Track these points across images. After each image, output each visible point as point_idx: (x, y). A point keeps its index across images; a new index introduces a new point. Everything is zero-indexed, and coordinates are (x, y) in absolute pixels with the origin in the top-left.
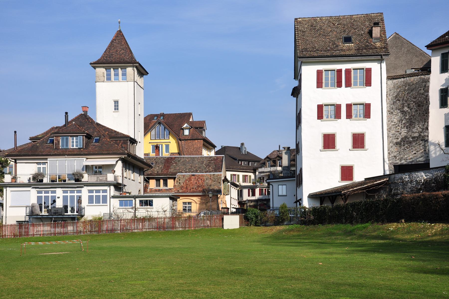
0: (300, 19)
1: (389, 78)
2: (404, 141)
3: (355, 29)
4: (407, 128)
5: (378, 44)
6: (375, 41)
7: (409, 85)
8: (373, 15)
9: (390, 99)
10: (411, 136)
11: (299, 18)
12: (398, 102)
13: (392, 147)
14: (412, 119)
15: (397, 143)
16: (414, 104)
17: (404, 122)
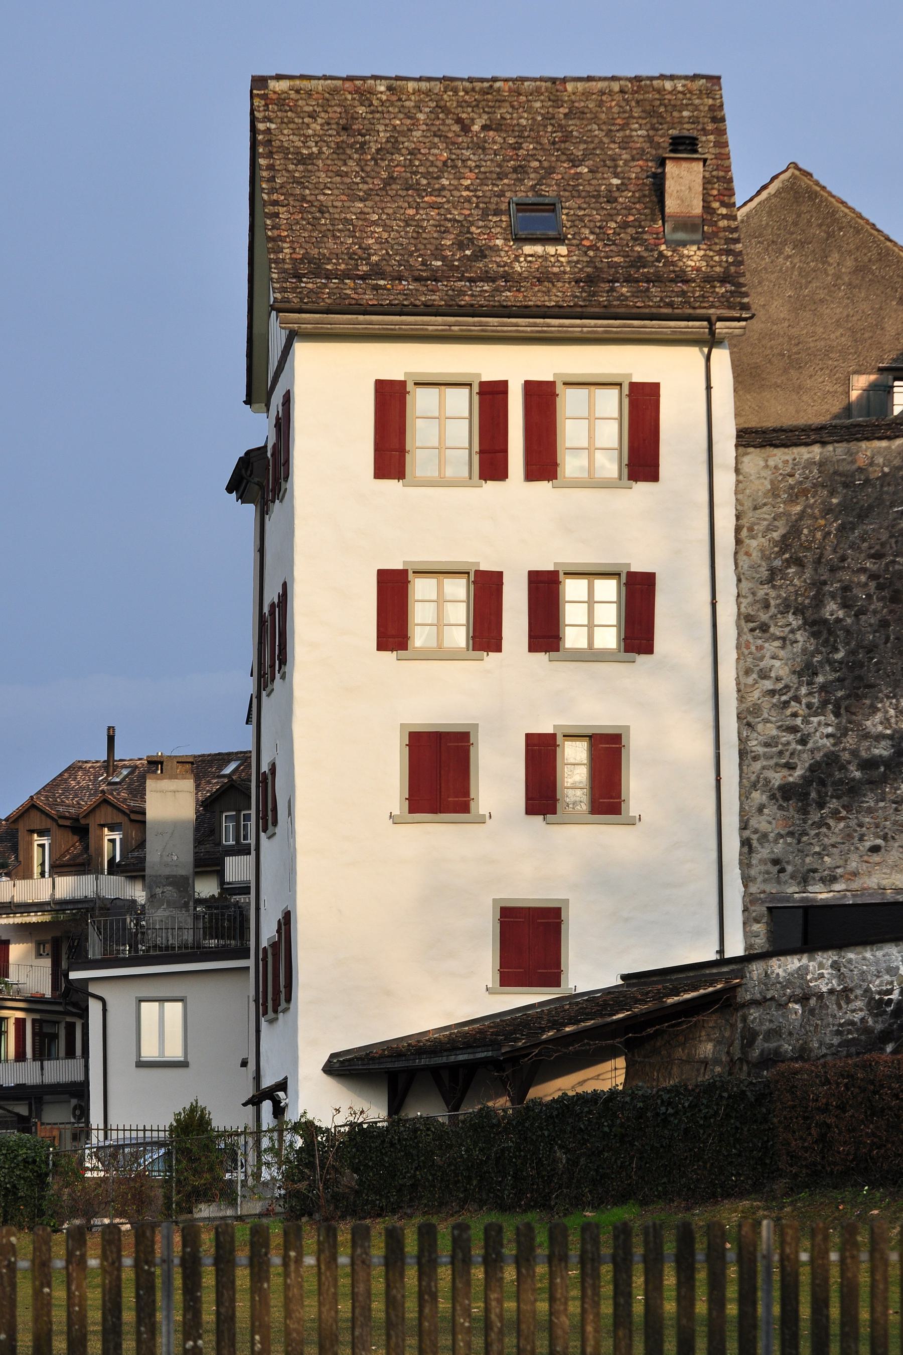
0: (283, 85)
1: (748, 438)
2: (822, 783)
3: (575, 162)
4: (837, 715)
5: (694, 257)
6: (681, 236)
7: (846, 485)
8: (668, 85)
9: (756, 555)
10: (855, 753)
11: (279, 77)
13: (760, 809)
15: (786, 792)
16: (872, 584)
17: (820, 679)
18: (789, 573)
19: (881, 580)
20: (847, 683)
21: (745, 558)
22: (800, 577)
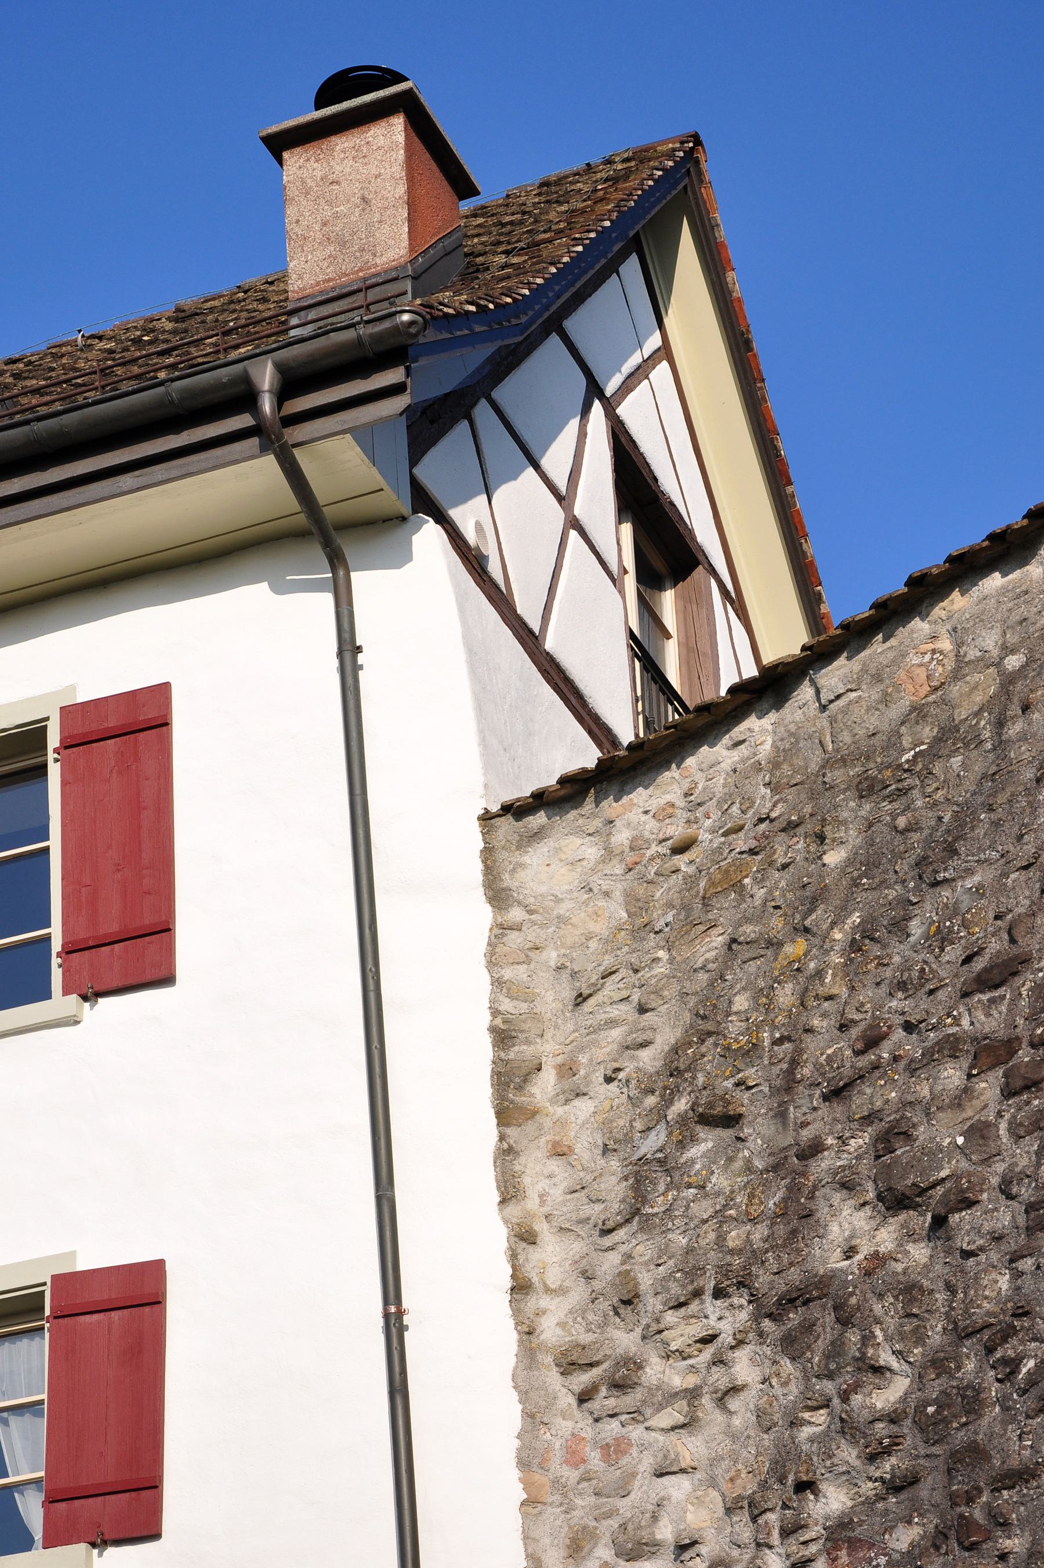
12: (707, 1142)
14: (972, 1401)
17: (833, 1500)
18: (693, 1161)
19: (1024, 1055)
20: (923, 1491)
21: (554, 1165)
22: (730, 1160)
